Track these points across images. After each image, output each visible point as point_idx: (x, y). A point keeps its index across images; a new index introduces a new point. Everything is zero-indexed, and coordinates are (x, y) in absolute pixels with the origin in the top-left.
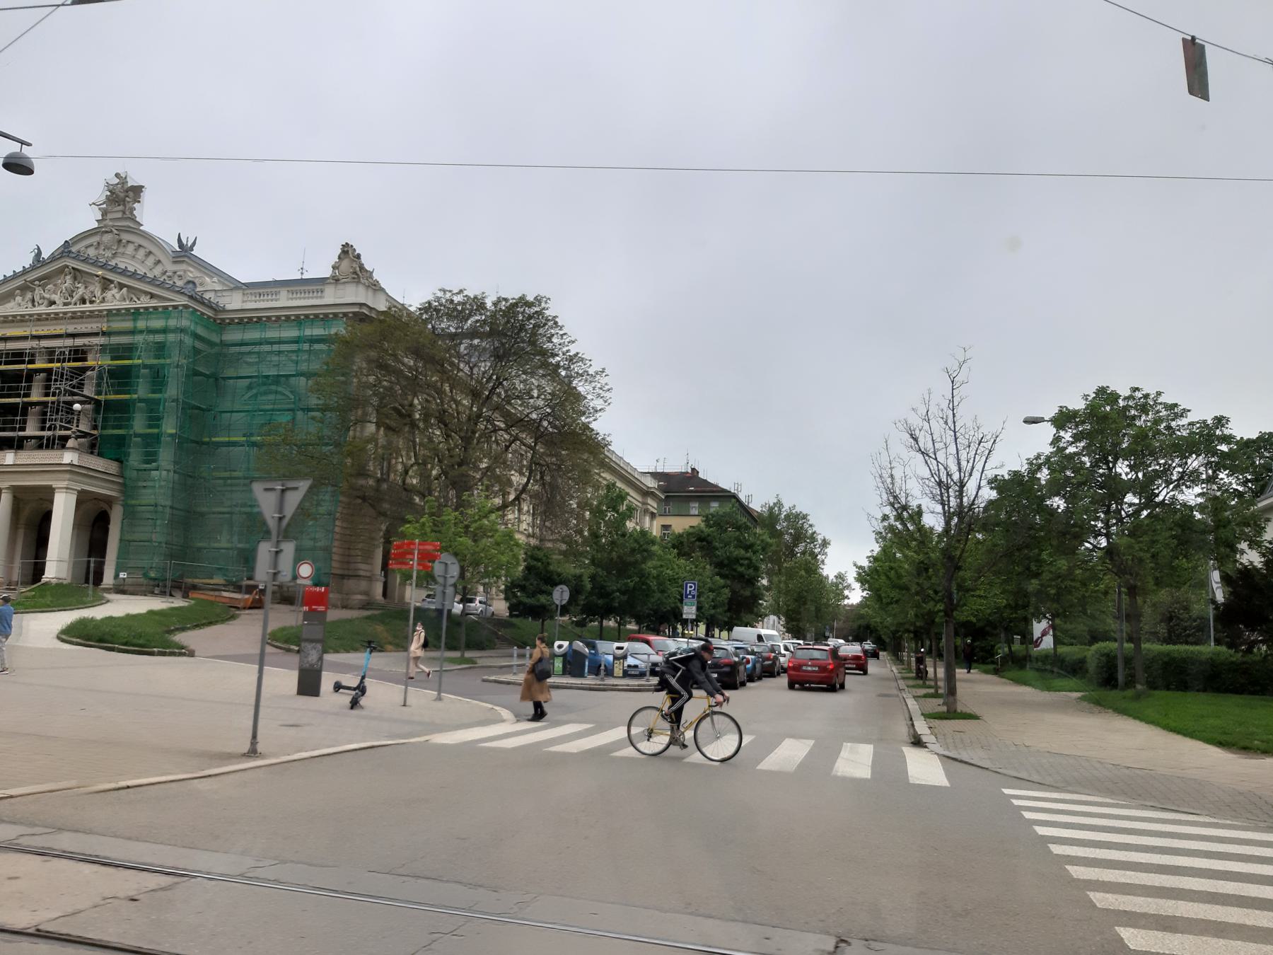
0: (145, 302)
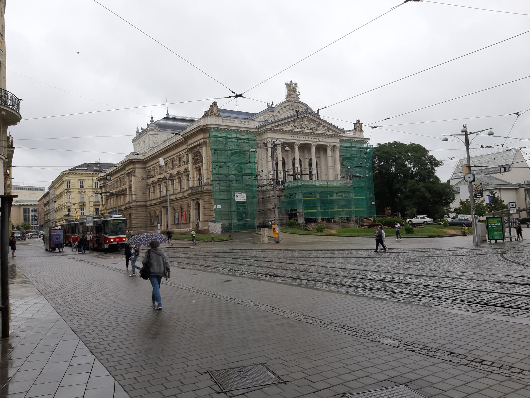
0: (331, 133)
